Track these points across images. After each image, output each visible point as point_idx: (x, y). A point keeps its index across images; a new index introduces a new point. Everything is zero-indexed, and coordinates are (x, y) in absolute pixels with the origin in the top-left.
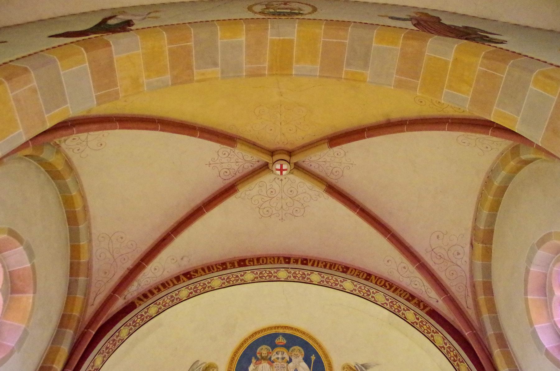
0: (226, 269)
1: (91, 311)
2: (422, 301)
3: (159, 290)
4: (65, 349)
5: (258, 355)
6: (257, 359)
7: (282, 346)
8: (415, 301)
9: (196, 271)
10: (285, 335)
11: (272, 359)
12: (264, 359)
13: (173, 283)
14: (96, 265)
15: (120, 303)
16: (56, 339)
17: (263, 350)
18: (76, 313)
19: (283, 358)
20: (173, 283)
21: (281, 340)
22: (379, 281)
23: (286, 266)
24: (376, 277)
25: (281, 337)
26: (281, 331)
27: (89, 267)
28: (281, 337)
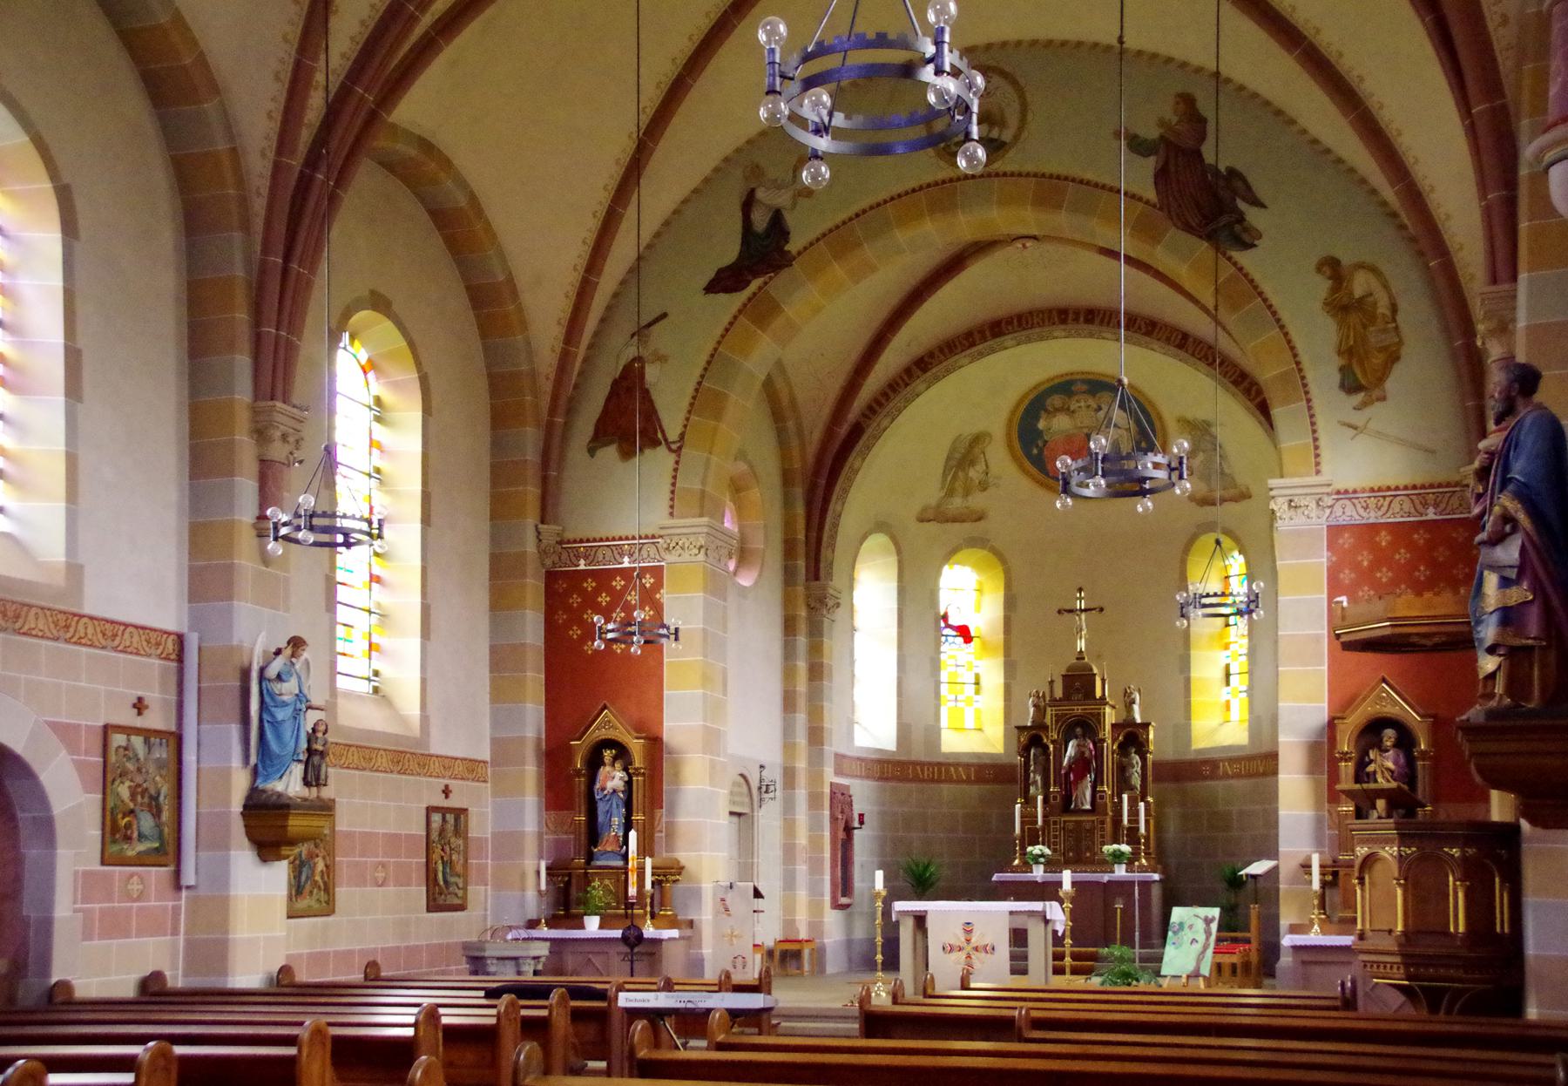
0: (973, 345)
1: (812, 450)
2: (1256, 384)
3: (888, 398)
4: (800, 510)
5: (1050, 408)
6: (1046, 410)
7: (1084, 392)
8: (1246, 384)
9: (931, 354)
10: (1084, 381)
11: (1072, 409)
12: (1057, 410)
13: (903, 380)
14: (801, 397)
15: (843, 430)
16: (787, 503)
17: (1056, 400)
18: (797, 465)
19: (1088, 407)
20: (903, 380)
21: (1079, 387)
22: (1199, 349)
23: (1063, 327)
24: (1195, 341)
25: (1079, 383)
26: (1078, 377)
27: (793, 401)
28: (1079, 383)
